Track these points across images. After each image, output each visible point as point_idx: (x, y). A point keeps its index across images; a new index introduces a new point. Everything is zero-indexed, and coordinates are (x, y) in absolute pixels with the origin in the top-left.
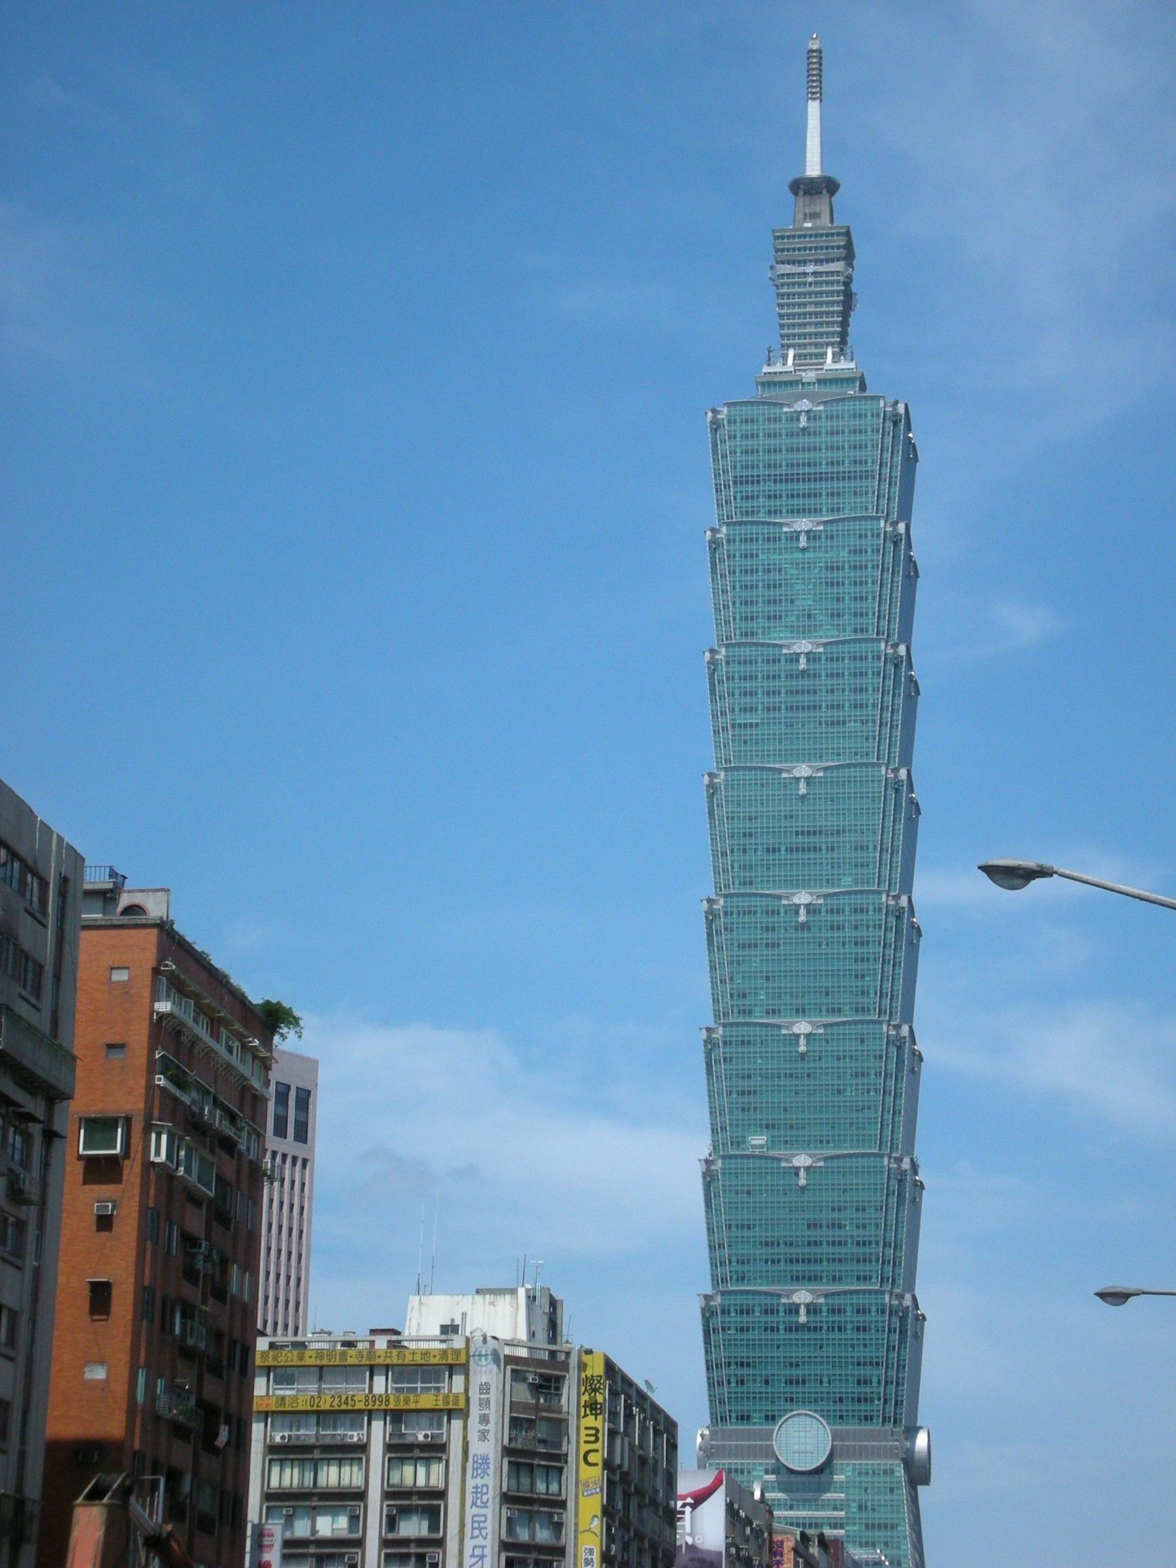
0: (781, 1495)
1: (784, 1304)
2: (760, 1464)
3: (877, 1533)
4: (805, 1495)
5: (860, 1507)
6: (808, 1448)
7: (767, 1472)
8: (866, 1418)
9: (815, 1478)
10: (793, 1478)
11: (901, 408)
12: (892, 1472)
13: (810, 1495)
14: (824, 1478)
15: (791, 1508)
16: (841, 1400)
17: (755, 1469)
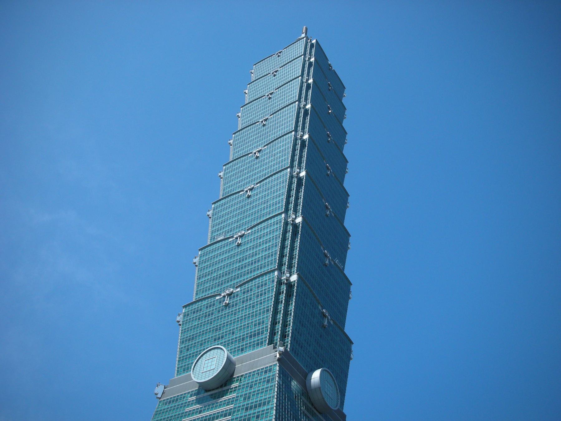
0: (198, 406)
1: (217, 300)
2: (189, 393)
3: (252, 411)
4: (210, 402)
5: (245, 399)
6: (213, 367)
7: (191, 396)
8: (258, 344)
9: (220, 390)
10: (206, 394)
11: (314, 41)
12: (270, 370)
13: (214, 401)
14: (225, 388)
15: (200, 412)
16: (243, 339)
17: (184, 397)
